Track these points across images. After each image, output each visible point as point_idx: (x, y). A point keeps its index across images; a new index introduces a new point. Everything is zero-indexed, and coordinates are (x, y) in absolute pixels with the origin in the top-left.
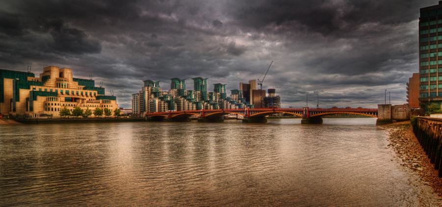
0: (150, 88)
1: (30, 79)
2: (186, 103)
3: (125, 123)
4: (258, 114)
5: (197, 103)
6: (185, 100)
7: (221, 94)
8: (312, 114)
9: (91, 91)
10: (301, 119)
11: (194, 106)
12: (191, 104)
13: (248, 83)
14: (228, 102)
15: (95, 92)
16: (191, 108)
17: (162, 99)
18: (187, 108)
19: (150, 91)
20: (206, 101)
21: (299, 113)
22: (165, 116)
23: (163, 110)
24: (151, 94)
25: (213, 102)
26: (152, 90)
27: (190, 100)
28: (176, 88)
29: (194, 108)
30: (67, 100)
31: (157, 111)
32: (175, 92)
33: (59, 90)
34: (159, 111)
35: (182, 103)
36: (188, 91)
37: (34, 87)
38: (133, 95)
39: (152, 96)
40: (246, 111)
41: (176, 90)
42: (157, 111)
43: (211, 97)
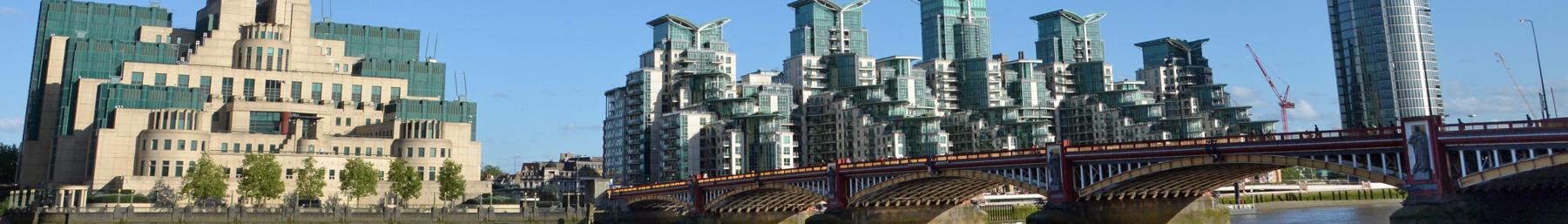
5: (911, 128)
8: (1472, 167)
9: (377, 82)
14: (1116, 114)
15: (396, 83)
36: (879, 64)
40: (1055, 160)
43: (1015, 90)
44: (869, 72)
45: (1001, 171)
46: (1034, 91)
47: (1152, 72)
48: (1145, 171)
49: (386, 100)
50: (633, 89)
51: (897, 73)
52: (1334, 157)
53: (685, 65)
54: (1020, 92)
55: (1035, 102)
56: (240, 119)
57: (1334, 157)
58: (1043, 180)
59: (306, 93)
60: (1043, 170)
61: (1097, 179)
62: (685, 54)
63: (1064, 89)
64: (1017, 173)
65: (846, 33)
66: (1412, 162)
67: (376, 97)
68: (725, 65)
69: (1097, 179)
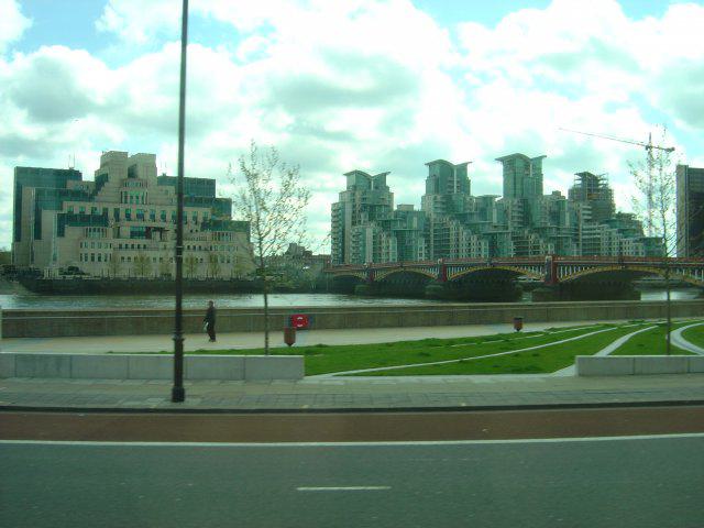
0: (358, 195)
1: (71, 185)
2: (464, 234)
6: (461, 228)
11: (485, 245)
12: (474, 239)
16: (474, 254)
17: (386, 225)
19: (358, 202)
20: (537, 230)
21: (681, 270)
23: (384, 257)
25: (554, 233)
30: (133, 235)
33: (122, 209)
35: (453, 237)
37: (70, 203)
39: (363, 217)
41: (439, 197)
49: (200, 220)
54: (558, 217)
55: (567, 224)
56: (126, 230)
59: (158, 216)
62: (365, 193)
65: (458, 182)
67: (195, 218)
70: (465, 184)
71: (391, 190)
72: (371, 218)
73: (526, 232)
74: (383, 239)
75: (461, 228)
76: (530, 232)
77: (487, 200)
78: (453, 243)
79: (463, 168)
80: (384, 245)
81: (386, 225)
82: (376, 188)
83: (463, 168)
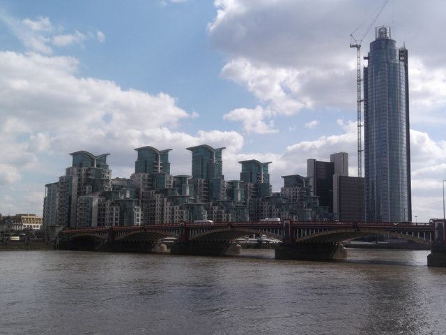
2: (167, 206)
3: (8, 253)
4: (315, 234)
6: (165, 200)
7: (256, 185)
10: (429, 252)
13: (329, 161)
18: (168, 220)
21: (422, 235)
22: (100, 236)
24: (85, 184)
26: (88, 175)
27: (174, 201)
28: (145, 172)
29: (184, 217)
31: (94, 224)
32: (144, 179)
34: (99, 225)
38: (46, 186)
41: (146, 175)
42: (94, 224)
44: (170, 182)
45: (262, 230)
46: (239, 197)
47: (288, 189)
48: (326, 233)
50: (64, 183)
51: (182, 183)
52: (404, 233)
53: (88, 175)
55: (239, 199)
57: (404, 233)
58: (280, 234)
60: (280, 230)
61: (304, 235)
62: (88, 170)
63: (252, 194)
64: (269, 231)
66: (436, 237)
68: (107, 175)
69: (304, 235)
70: (166, 166)
71: (110, 168)
72: (94, 191)
73: (211, 204)
74: (108, 207)
75: (165, 200)
76: (214, 205)
77: (181, 179)
78: (158, 212)
79: (165, 154)
80: (108, 212)
81: (106, 195)
82: (98, 166)
83: (165, 154)
